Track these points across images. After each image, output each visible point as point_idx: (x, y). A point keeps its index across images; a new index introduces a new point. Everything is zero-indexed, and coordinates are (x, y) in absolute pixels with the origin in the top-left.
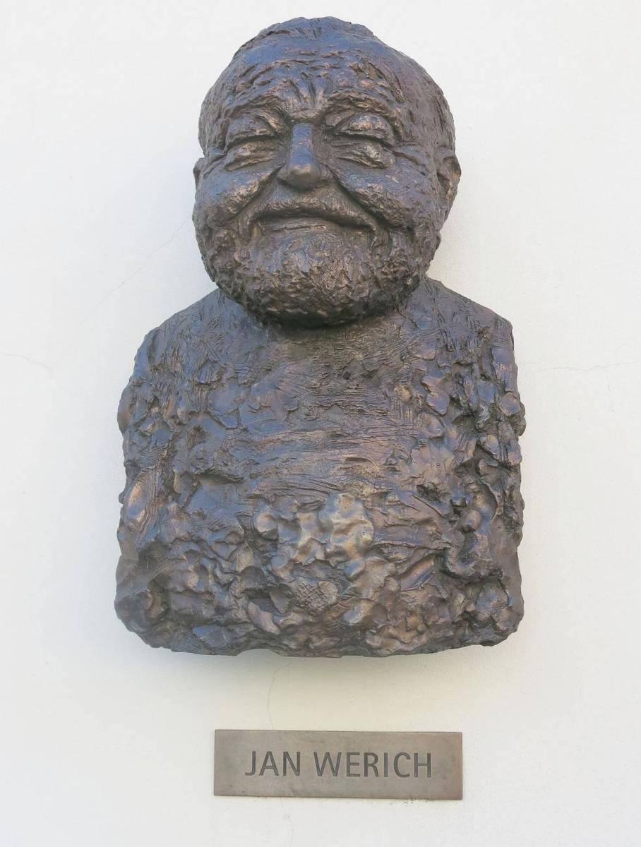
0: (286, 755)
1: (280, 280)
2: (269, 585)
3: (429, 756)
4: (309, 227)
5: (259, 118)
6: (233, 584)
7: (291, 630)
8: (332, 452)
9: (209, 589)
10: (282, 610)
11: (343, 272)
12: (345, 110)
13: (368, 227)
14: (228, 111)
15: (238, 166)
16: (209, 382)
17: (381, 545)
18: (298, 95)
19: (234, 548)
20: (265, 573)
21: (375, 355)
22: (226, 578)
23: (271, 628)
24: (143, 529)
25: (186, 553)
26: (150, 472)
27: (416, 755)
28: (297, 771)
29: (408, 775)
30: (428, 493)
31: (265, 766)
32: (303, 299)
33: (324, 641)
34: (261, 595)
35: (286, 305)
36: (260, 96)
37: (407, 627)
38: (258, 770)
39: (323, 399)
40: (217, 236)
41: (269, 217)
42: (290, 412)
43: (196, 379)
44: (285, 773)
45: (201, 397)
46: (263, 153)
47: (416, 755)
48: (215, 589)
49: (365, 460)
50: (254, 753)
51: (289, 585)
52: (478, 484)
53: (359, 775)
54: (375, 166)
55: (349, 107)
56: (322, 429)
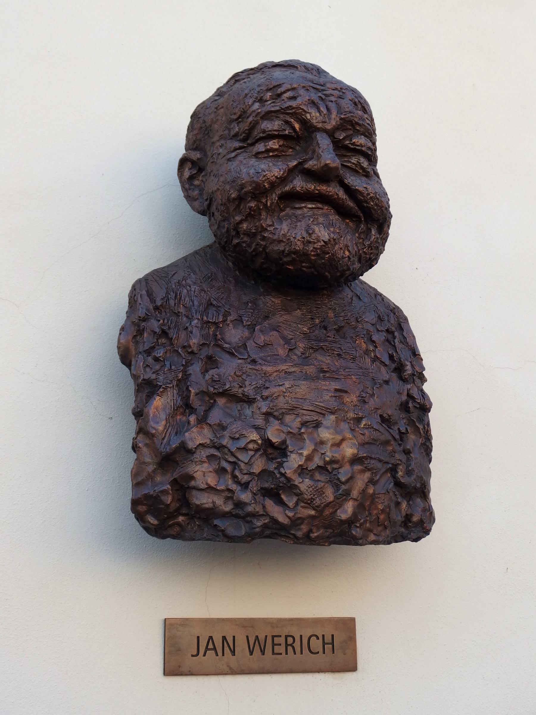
0: (224, 638)
1: (304, 244)
2: (281, 485)
3: (333, 636)
4: (322, 209)
5: (287, 122)
6: (251, 483)
7: (299, 521)
8: (324, 383)
9: (230, 487)
10: (291, 504)
11: (347, 246)
12: (347, 129)
13: (359, 217)
14: (259, 113)
15: (266, 155)
16: (217, 321)
17: (363, 457)
18: (318, 109)
19: (252, 453)
20: (278, 476)
21: (341, 315)
22: (246, 478)
23: (282, 519)
24: (165, 437)
25: (208, 457)
26: (169, 389)
27: (323, 636)
28: (233, 653)
29: (318, 652)
30: (385, 420)
31: (207, 649)
32: (320, 262)
33: (321, 531)
34: (273, 494)
35: (304, 264)
36: (290, 106)
37: (379, 522)
38: (202, 650)
39: (313, 342)
40: (249, 205)
41: (292, 198)
42: (290, 349)
43: (205, 318)
44: (223, 655)
45: (209, 333)
46: (285, 149)
47: (323, 636)
48: (234, 487)
49: (346, 392)
50: (198, 637)
51: (299, 485)
52: (408, 419)
53: (281, 654)
54: (364, 174)
55: (350, 127)
56: (314, 365)
